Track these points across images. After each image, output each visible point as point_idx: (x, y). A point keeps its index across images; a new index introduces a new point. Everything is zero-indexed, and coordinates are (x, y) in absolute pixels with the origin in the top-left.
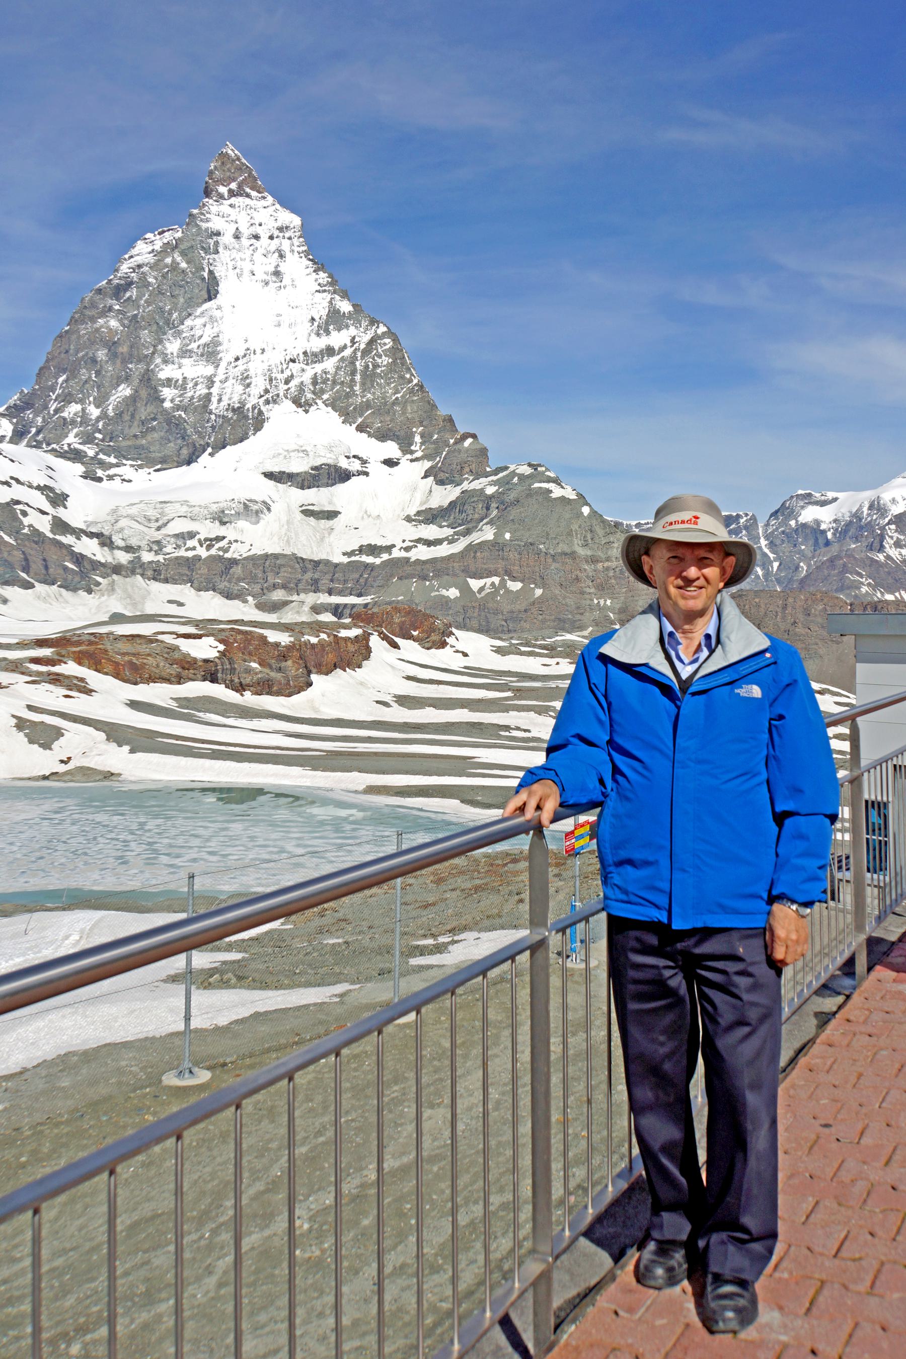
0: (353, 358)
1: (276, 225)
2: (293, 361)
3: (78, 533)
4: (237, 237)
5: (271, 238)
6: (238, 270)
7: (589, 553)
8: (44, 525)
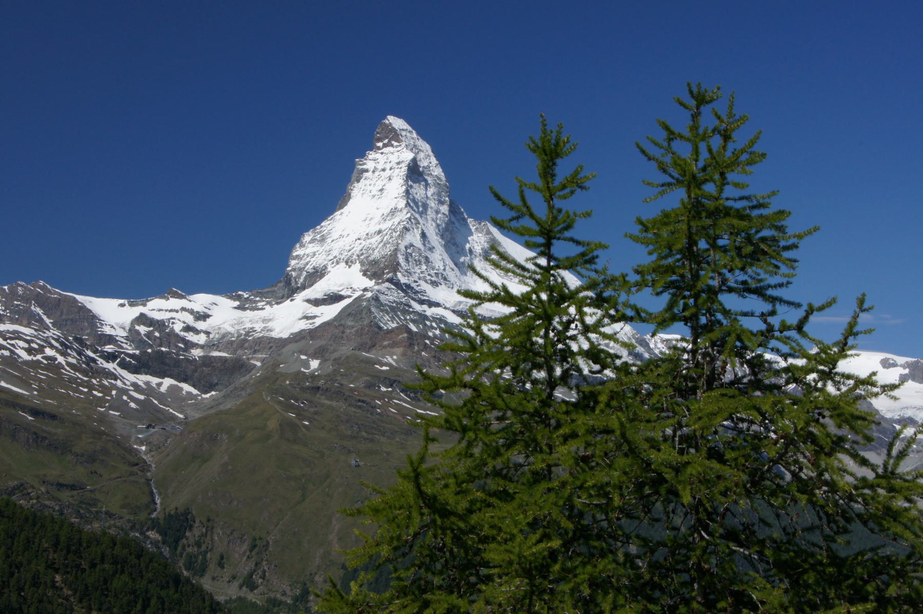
3: (197, 332)
4: (374, 172)
5: (391, 169)
7: (353, 323)
8: (178, 328)
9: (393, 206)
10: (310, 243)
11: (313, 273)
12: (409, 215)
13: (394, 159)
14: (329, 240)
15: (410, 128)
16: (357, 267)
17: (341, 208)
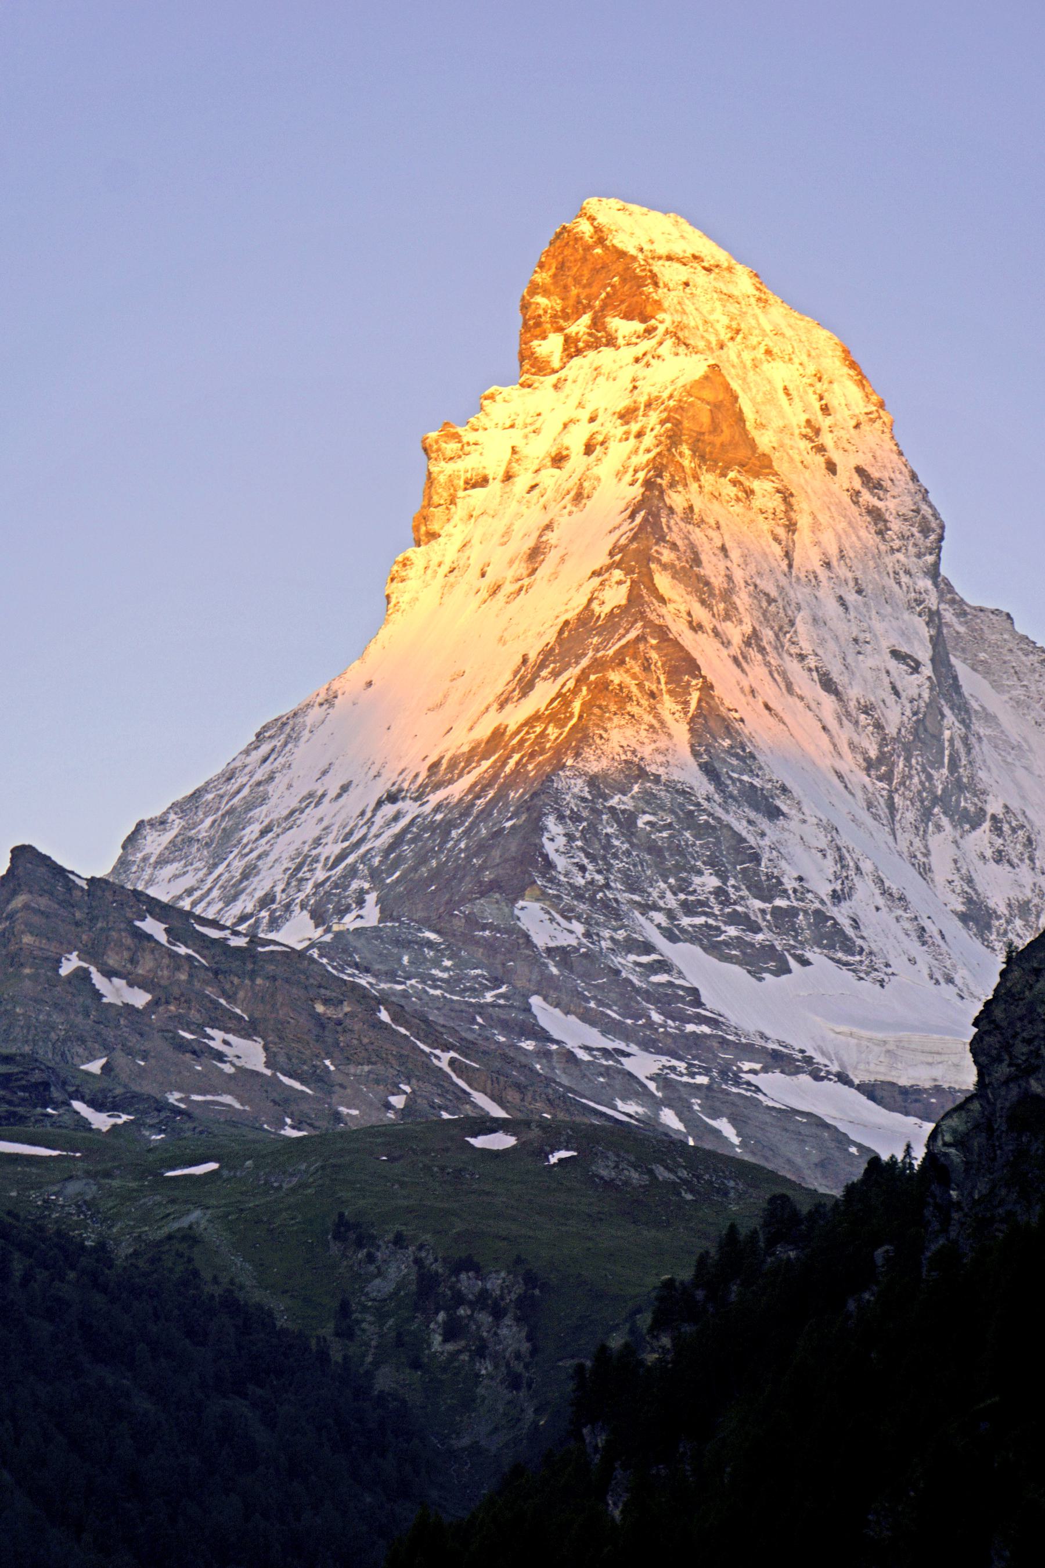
0: (522, 741)
1: (623, 403)
2: (392, 798)
4: (508, 477)
5: (589, 449)
6: (452, 578)
10: (162, 862)
13: (610, 397)
14: (252, 831)
15: (722, 257)
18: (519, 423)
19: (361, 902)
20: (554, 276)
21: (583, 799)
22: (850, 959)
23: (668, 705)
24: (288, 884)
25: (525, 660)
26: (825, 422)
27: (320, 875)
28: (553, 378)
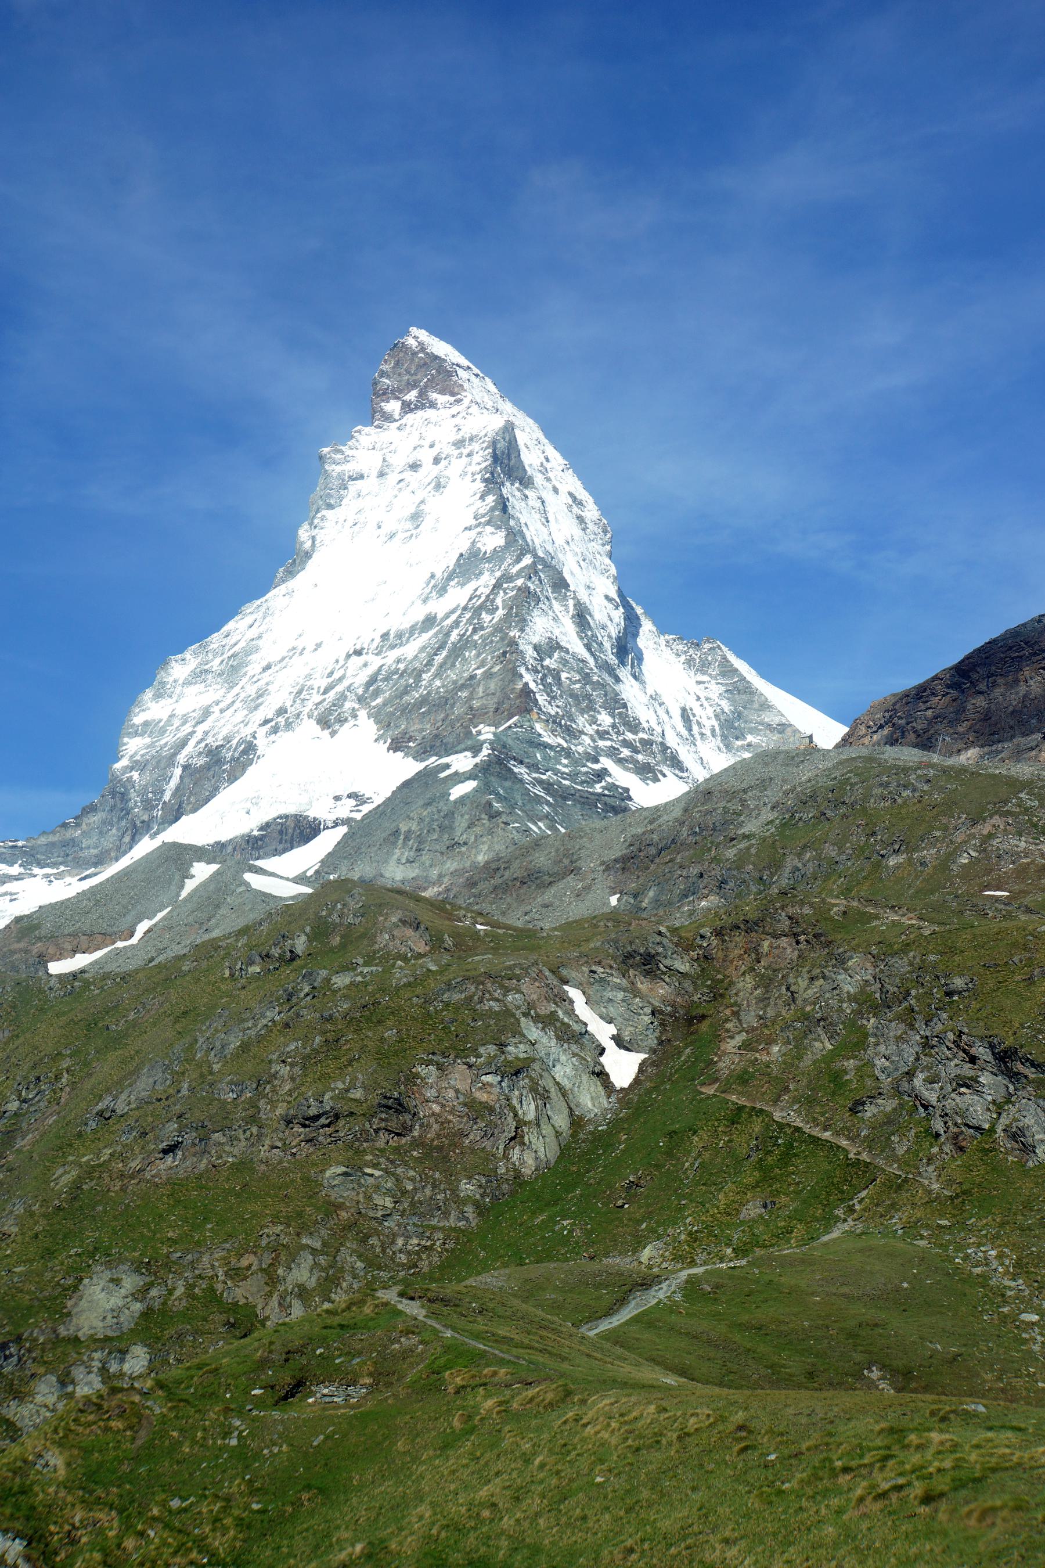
0: (457, 623)
1: (455, 437)
2: (358, 653)
4: (381, 474)
5: (437, 461)
9: (464, 546)
10: (186, 683)
11: (207, 767)
12: (527, 560)
14: (254, 667)
16: (365, 727)
17: (291, 573)
18: (378, 446)
19: (355, 716)
20: (393, 367)
21: (535, 659)
22: (681, 774)
23: (556, 605)
24: (294, 702)
25: (433, 576)
26: (548, 466)
27: (317, 698)
28: (397, 424)
